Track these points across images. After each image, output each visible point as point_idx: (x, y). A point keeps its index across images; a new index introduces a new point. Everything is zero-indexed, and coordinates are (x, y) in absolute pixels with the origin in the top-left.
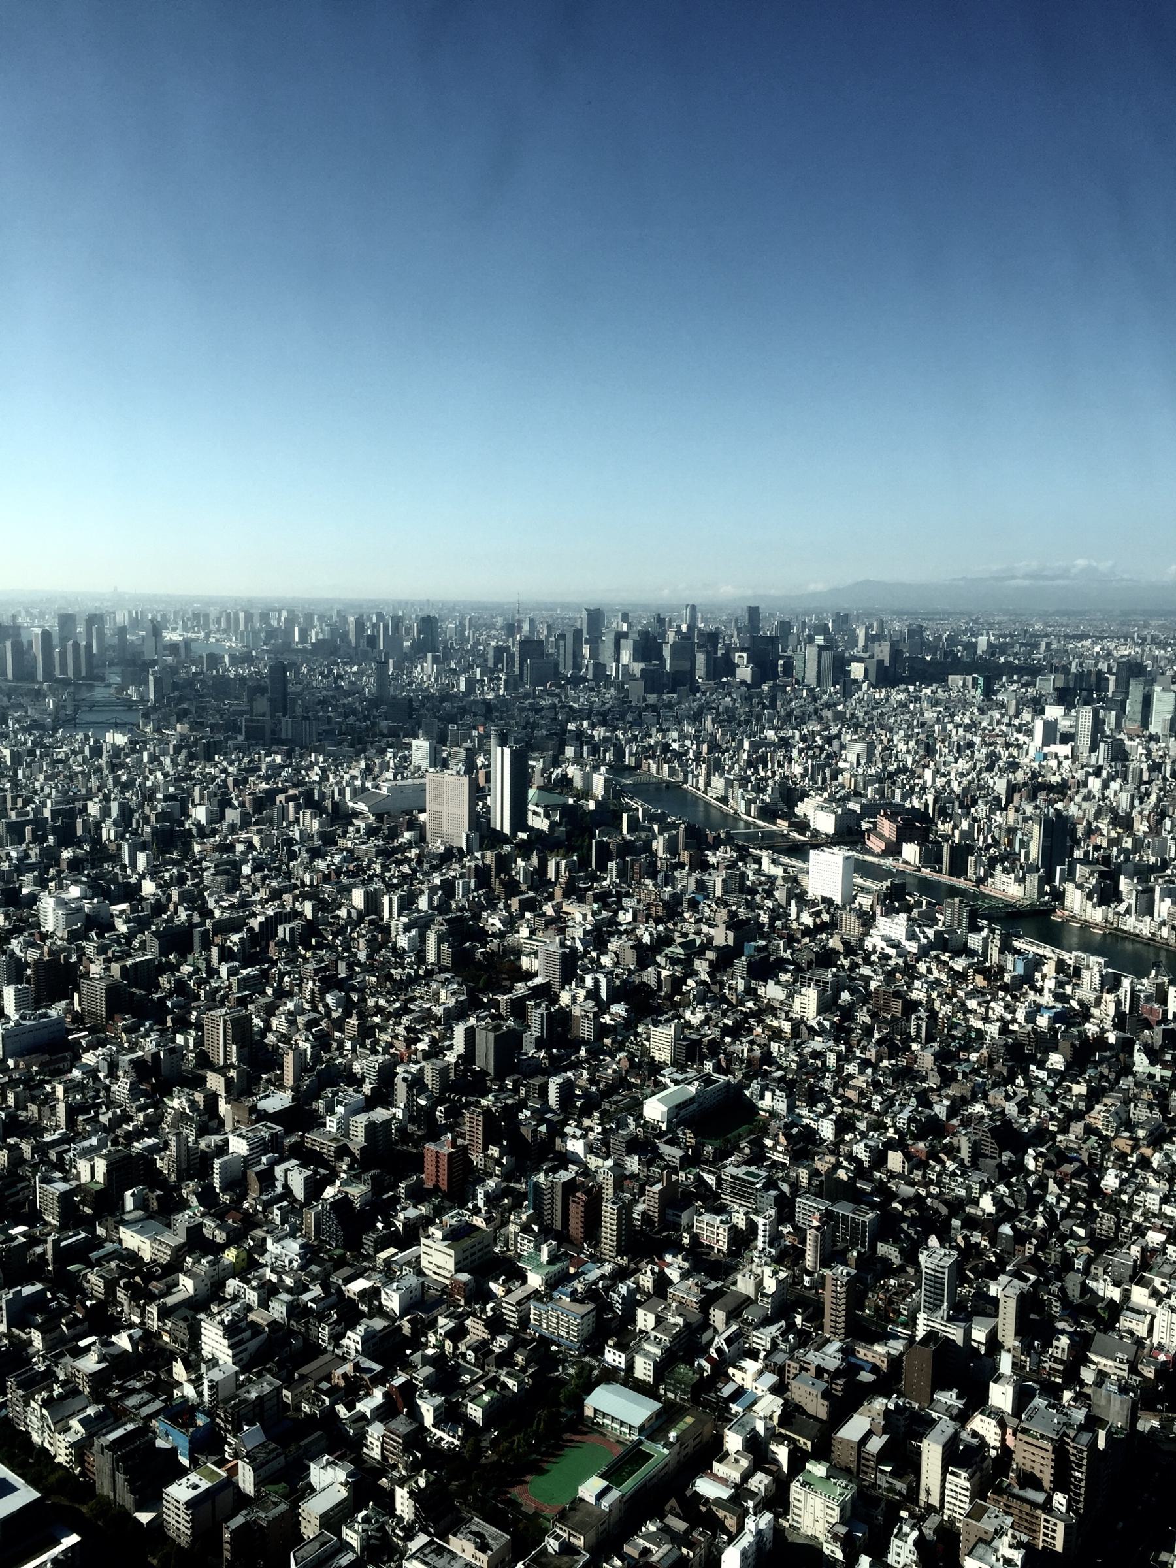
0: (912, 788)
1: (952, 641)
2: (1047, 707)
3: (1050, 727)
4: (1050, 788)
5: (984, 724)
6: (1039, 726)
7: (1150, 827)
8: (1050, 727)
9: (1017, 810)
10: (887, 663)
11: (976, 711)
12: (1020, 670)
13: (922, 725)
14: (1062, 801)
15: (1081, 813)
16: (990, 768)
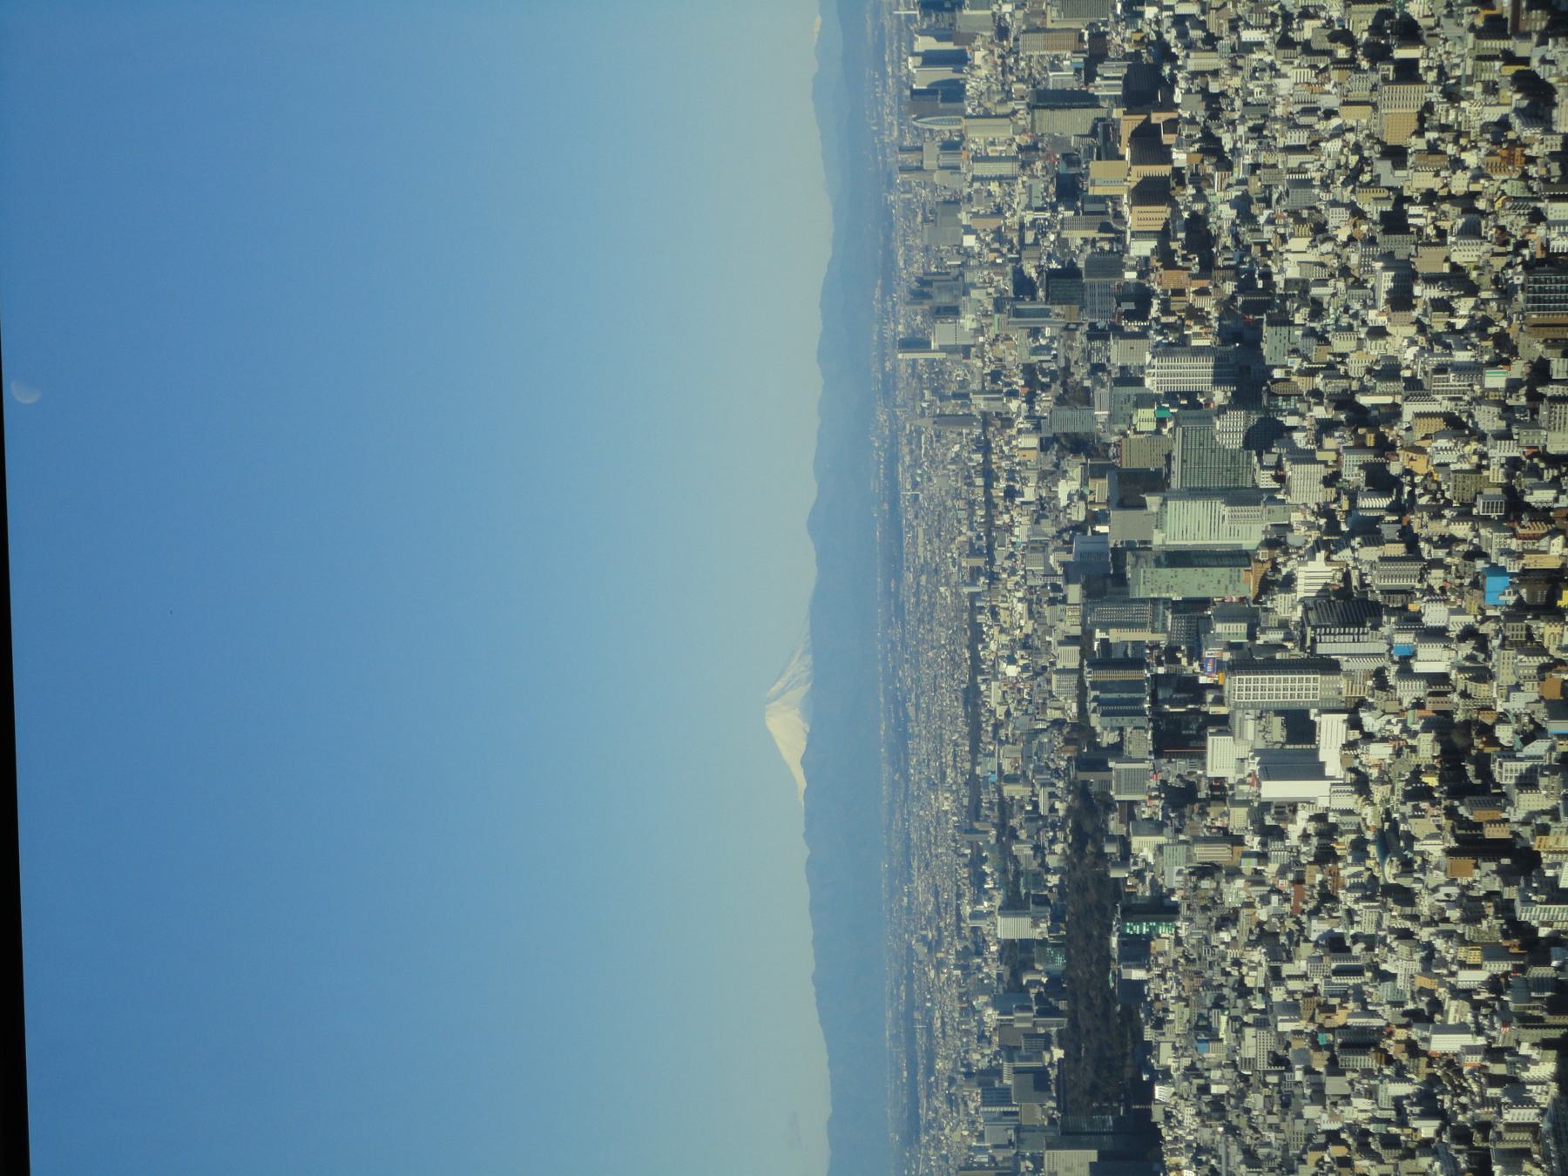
0: (1495, 1081)
1: (1011, 994)
2: (1210, 774)
3: (1274, 765)
4: (1452, 758)
5: (1262, 914)
6: (1274, 790)
7: (1553, 534)
8: (1274, 765)
9: (1544, 830)
10: (1093, 1155)
11: (1225, 936)
12: (1081, 839)
13: (1280, 1062)
14: (1487, 732)
15: (1528, 686)
16: (1405, 897)
